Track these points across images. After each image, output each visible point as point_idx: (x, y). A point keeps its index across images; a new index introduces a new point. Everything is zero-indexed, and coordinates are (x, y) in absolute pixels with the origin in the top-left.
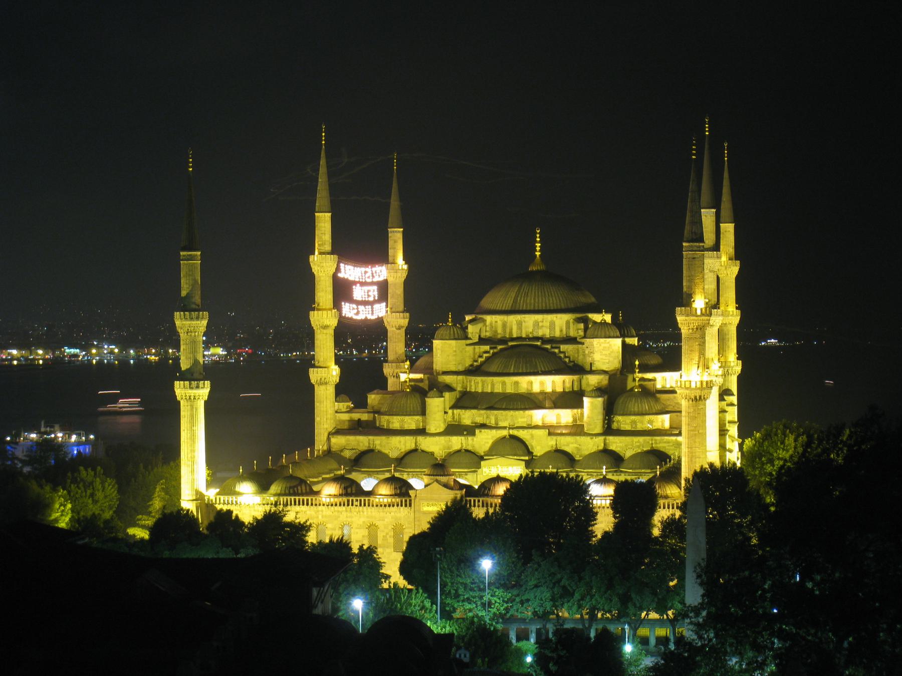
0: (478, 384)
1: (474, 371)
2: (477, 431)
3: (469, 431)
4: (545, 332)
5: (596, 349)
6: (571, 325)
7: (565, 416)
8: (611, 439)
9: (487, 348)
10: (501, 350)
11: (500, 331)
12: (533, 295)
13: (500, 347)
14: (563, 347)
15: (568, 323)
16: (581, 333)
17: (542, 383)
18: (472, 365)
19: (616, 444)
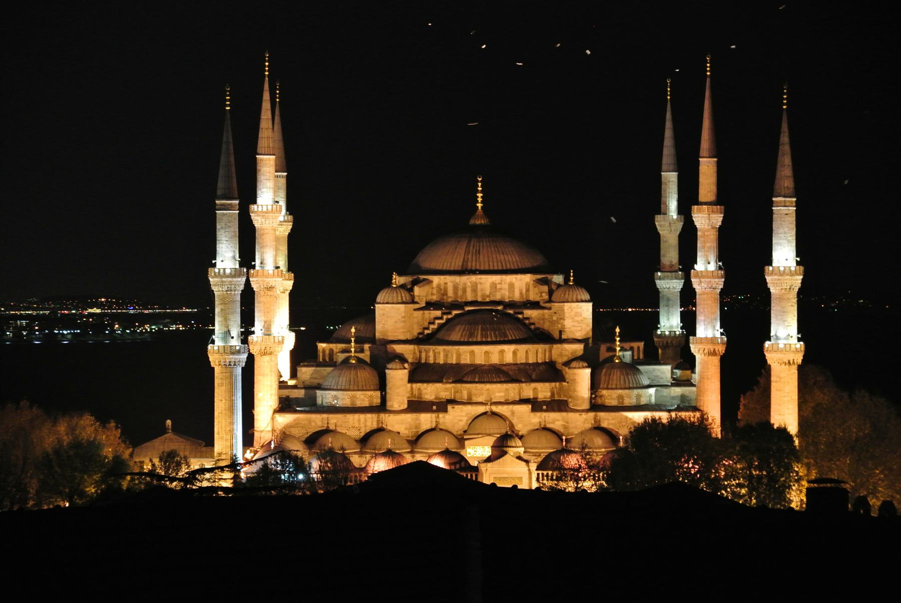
0: (439, 354)
1: (422, 340)
2: (449, 407)
3: (441, 406)
4: (504, 294)
5: (567, 315)
6: (531, 287)
7: (543, 391)
8: (602, 415)
9: (438, 313)
10: (456, 315)
11: (450, 293)
12: (489, 255)
13: (455, 312)
14: (528, 313)
15: (527, 285)
16: (546, 297)
17: (515, 353)
18: (422, 333)
19: (608, 420)
